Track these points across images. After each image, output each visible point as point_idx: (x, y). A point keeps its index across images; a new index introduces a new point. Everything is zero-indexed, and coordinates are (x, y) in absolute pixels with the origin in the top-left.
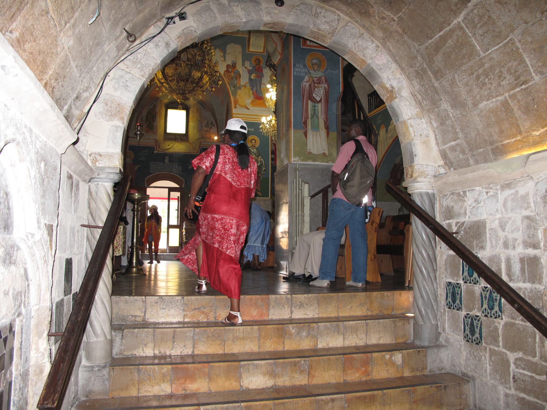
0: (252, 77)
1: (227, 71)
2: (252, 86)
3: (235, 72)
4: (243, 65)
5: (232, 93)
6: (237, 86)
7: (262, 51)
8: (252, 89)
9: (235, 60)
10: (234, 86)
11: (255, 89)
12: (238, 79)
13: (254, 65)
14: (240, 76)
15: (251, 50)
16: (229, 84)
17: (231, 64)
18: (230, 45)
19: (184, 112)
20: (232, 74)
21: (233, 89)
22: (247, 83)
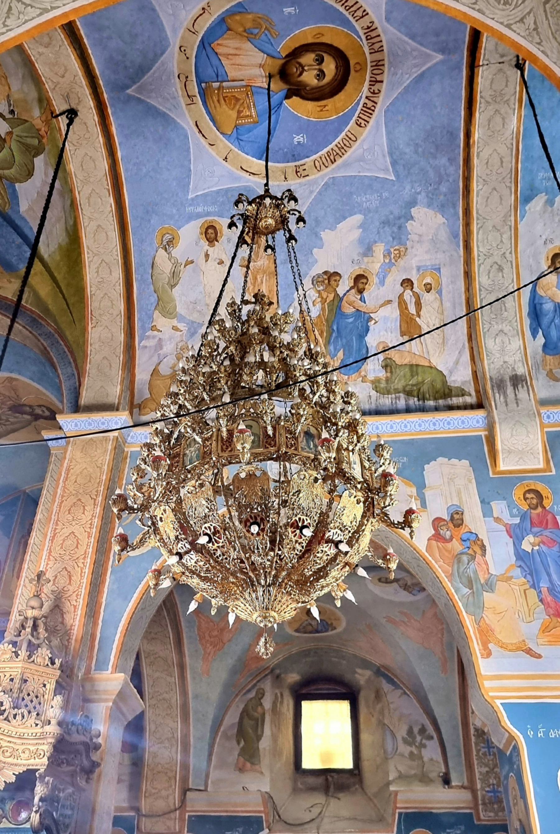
0: (526, 546)
1: (437, 537)
2: (531, 574)
3: (465, 537)
4: (487, 512)
5: (466, 606)
6: (477, 579)
7: (541, 466)
8: (533, 586)
9: (456, 502)
10: (470, 584)
11: (544, 585)
12: (478, 557)
13: (525, 508)
14: (483, 548)
15: (502, 466)
16: (450, 577)
17: (446, 517)
18: (433, 463)
19: (344, 706)
20: (456, 546)
21: (466, 590)
22: (512, 566)
